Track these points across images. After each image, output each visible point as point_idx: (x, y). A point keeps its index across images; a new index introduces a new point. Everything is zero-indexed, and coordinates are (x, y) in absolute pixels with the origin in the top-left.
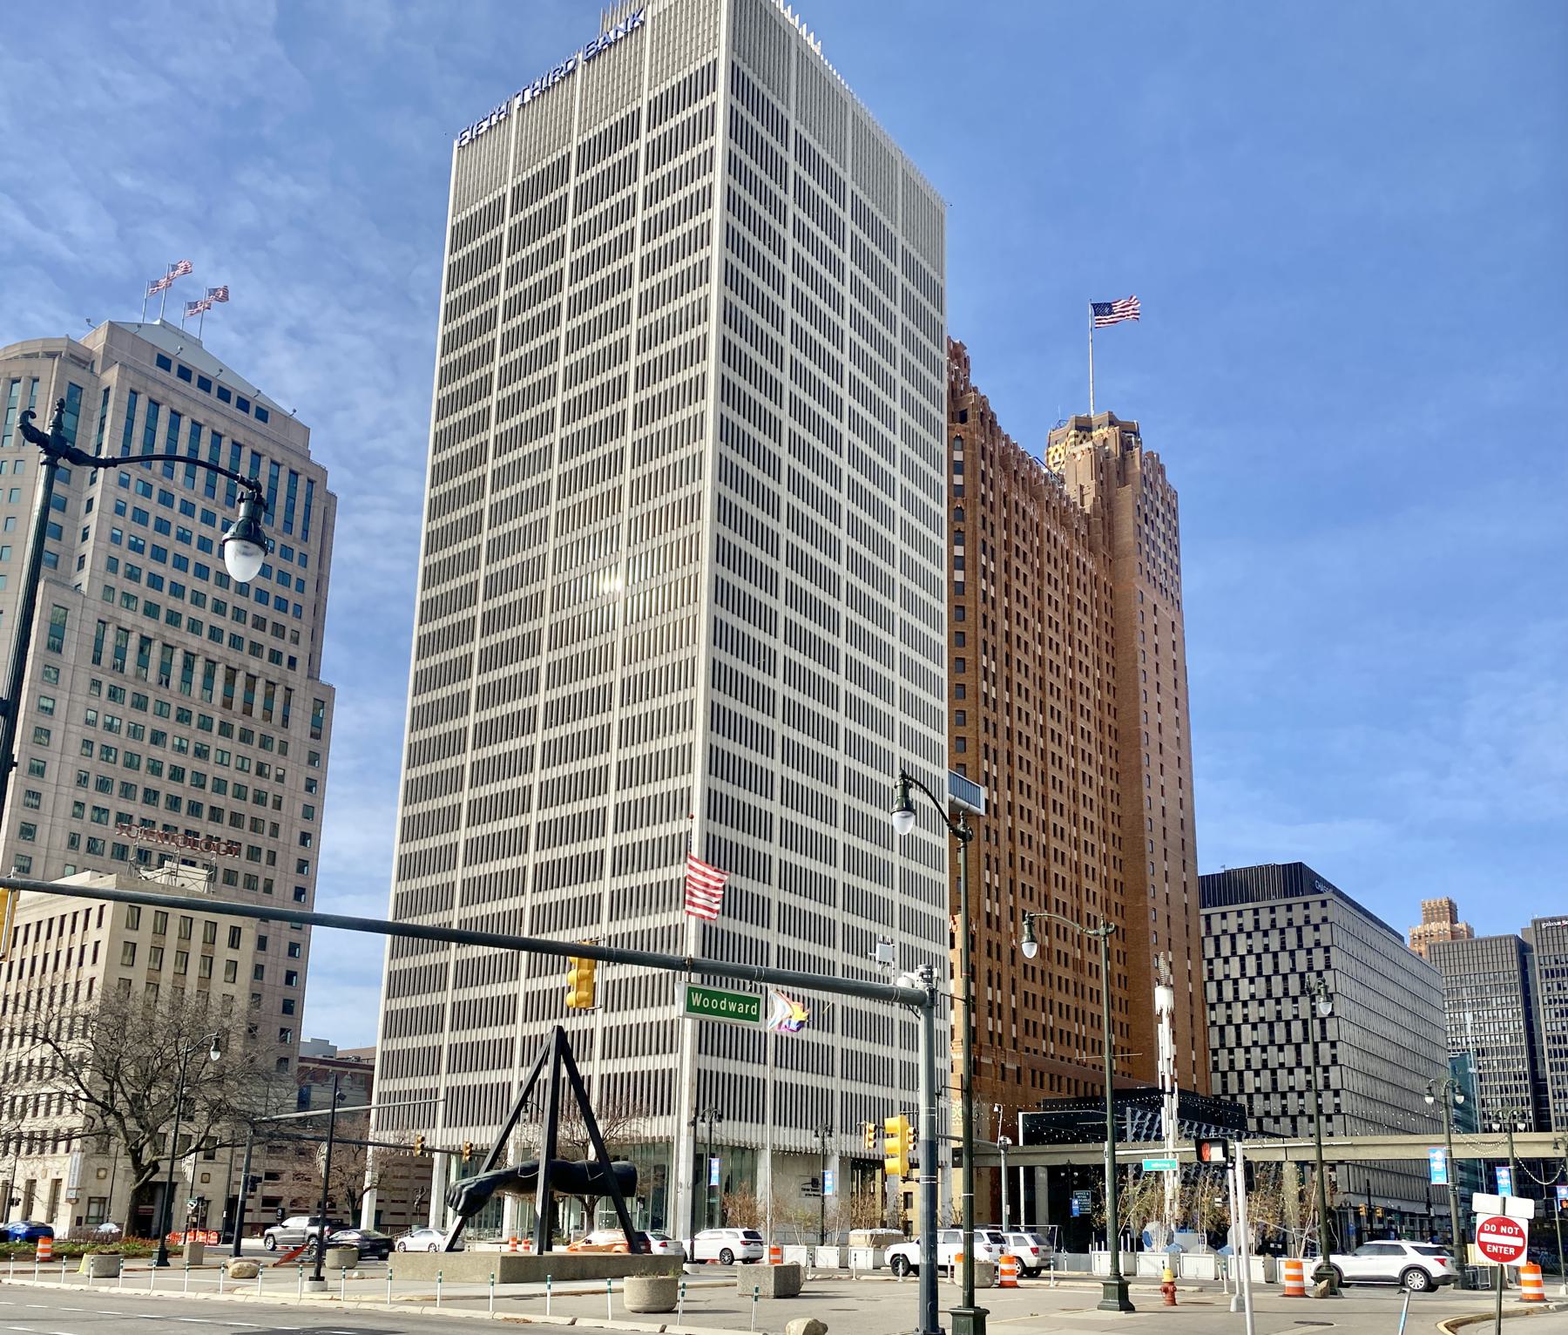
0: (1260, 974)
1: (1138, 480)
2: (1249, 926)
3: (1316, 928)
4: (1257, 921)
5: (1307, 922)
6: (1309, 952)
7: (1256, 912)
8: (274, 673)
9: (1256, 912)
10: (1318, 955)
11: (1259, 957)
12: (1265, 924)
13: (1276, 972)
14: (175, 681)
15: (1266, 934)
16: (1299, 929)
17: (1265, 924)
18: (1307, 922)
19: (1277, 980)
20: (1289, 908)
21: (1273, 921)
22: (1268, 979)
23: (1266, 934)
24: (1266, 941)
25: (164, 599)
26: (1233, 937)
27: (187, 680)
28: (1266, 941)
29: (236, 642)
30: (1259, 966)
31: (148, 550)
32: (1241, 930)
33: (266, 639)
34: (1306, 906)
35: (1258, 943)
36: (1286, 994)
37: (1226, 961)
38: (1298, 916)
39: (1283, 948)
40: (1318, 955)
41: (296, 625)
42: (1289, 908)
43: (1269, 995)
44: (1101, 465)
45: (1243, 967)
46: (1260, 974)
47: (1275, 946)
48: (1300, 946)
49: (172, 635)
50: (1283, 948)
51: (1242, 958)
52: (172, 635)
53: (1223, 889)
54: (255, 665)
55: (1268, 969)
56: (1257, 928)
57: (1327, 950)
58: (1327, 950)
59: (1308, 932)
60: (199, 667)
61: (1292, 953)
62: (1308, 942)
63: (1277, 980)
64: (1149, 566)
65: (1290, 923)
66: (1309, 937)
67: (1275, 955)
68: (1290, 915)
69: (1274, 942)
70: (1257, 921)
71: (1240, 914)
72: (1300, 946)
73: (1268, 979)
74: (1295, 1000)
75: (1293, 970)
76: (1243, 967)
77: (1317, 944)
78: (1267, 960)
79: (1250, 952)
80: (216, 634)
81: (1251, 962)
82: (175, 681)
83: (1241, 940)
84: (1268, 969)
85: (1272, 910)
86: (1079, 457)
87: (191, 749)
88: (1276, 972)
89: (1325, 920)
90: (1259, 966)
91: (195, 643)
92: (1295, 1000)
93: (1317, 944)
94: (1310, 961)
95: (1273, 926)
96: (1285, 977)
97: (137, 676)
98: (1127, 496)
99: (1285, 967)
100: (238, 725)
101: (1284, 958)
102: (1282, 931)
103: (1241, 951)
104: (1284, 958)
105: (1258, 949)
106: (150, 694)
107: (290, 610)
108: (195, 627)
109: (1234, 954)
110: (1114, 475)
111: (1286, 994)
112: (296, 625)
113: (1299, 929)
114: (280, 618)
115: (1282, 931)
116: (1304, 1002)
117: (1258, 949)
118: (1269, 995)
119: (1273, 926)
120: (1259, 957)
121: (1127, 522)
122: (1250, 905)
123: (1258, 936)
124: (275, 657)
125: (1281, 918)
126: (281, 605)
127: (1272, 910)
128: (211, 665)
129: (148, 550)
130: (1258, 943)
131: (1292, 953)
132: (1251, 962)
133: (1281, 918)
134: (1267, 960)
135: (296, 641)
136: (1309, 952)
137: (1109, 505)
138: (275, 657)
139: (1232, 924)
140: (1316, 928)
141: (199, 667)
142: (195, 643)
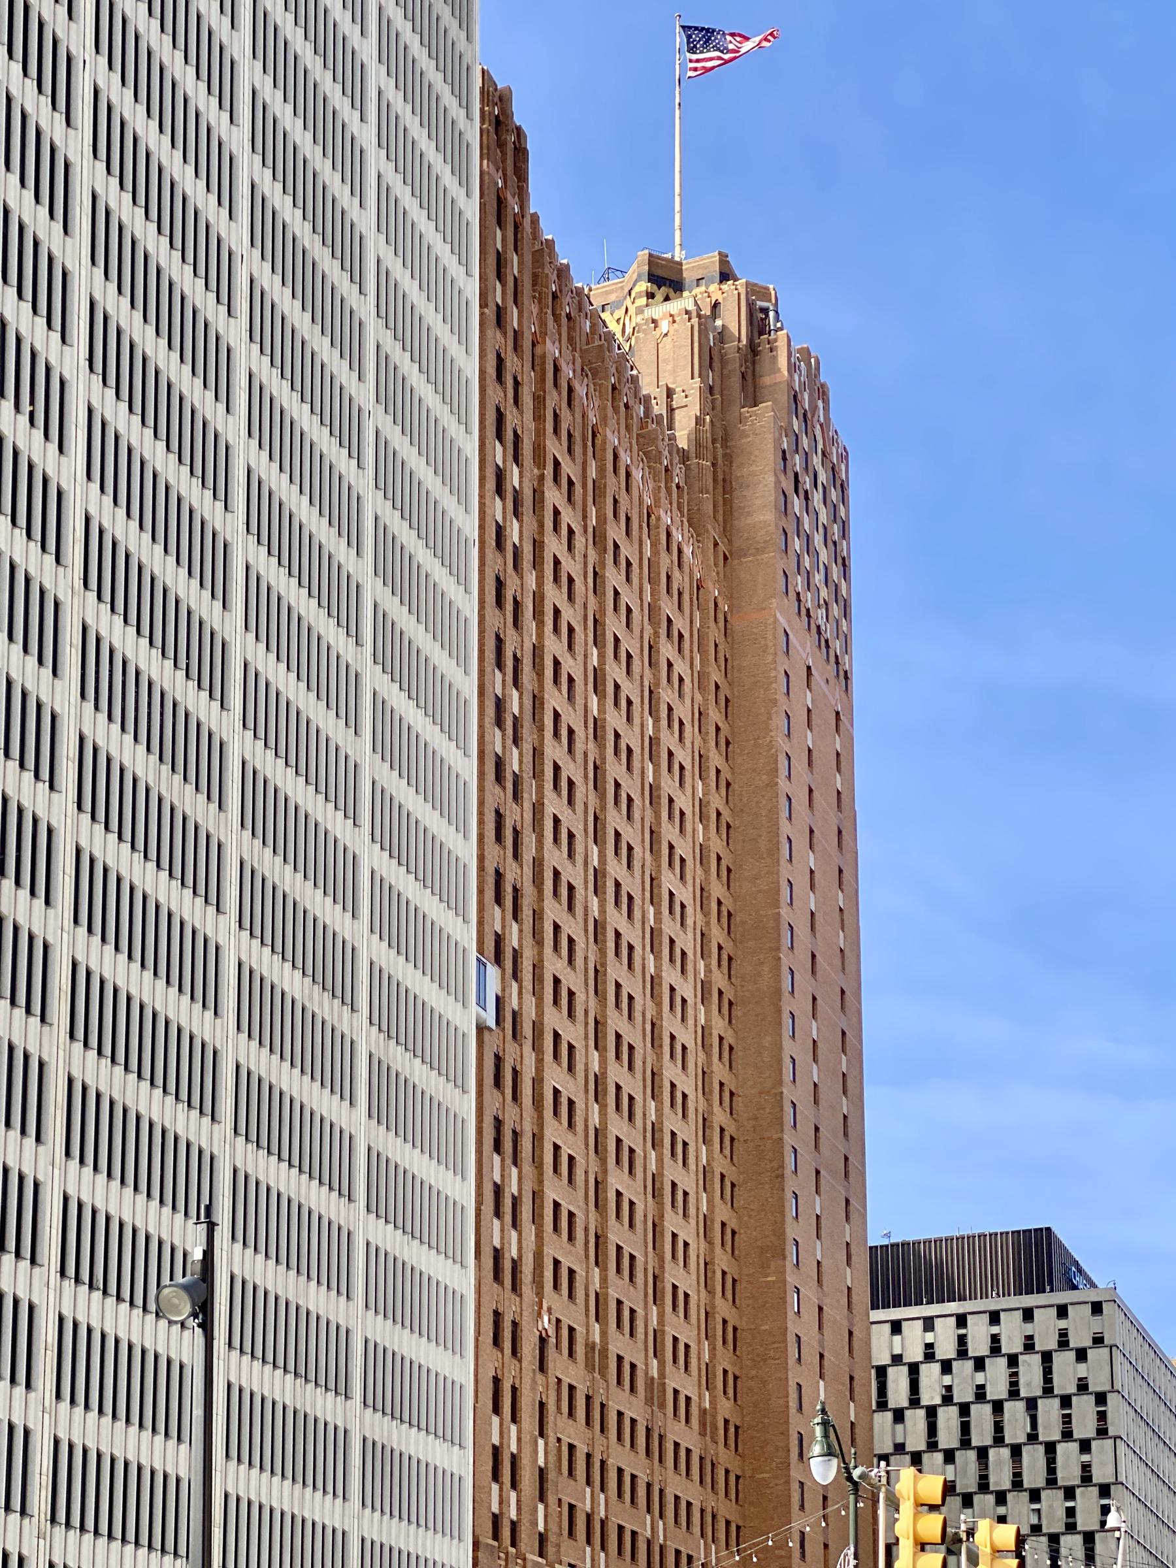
0: (965, 1443)
1: (784, 398)
2: (946, 1349)
3: (1081, 1355)
4: (962, 1340)
5: (1063, 1343)
6: (1066, 1401)
7: (961, 1321)
9: (961, 1321)
10: (1084, 1408)
11: (964, 1409)
12: (978, 1345)
13: (999, 1440)
15: (980, 1364)
16: (1047, 1357)
17: (978, 1345)
18: (1063, 1343)
19: (1000, 1457)
20: (1028, 1315)
21: (995, 1339)
22: (982, 1453)
23: (980, 1364)
24: (980, 1378)
26: (914, 1369)
28: (980, 1378)
30: (965, 1428)
32: (929, 1356)
34: (1062, 1311)
35: (964, 1380)
36: (1017, 1484)
37: (899, 1416)
38: (1045, 1329)
39: (1014, 1393)
40: (1084, 1408)
42: (1028, 1315)
43: (984, 1487)
44: (711, 354)
45: (932, 1430)
46: (965, 1443)
47: (998, 1389)
48: (1048, 1391)
50: (1014, 1393)
51: (931, 1412)
53: (903, 1276)
55: (982, 1434)
56: (962, 1353)
57: (1101, 1398)
58: (1101, 1398)
59: (1064, 1362)
61: (1032, 1404)
62: (1064, 1383)
63: (1000, 1457)
64: (799, 582)
65: (1029, 1346)
66: (1066, 1372)
67: (998, 1407)
68: (1029, 1329)
69: (996, 1378)
70: (962, 1340)
71: (929, 1324)
72: (1048, 1391)
73: (982, 1453)
74: (1035, 1495)
75: (1033, 1438)
76: (932, 1430)
77: (1083, 1386)
78: (982, 1415)
79: (947, 1399)
81: (948, 1418)
83: (930, 1374)
84: (982, 1434)
85: (995, 1318)
86: (664, 326)
88: (999, 1440)
89: (1098, 1341)
90: (965, 1428)
92: (1035, 1495)
93: (1083, 1386)
94: (1067, 1419)
95: (995, 1350)
96: (1016, 1451)
98: (762, 426)
99: (1016, 1431)
101: (1015, 1412)
102: (1013, 1360)
103: (930, 1395)
104: (1015, 1412)
105: (964, 1394)
109: (915, 1402)
110: (735, 381)
111: (1017, 1484)
113: (1047, 1357)
115: (1013, 1360)
116: (1053, 1502)
117: (964, 1394)
118: (984, 1487)
119: (995, 1350)
120: (964, 1409)
121: (761, 483)
122: (954, 1307)
123: (963, 1368)
125: (1012, 1333)
127: (995, 1318)
130: (964, 1380)
131: (1032, 1404)
132: (948, 1418)
133: (1012, 1333)
134: (982, 1415)
136: (1066, 1401)
137: (726, 439)
139: (912, 1344)
140: (1081, 1355)
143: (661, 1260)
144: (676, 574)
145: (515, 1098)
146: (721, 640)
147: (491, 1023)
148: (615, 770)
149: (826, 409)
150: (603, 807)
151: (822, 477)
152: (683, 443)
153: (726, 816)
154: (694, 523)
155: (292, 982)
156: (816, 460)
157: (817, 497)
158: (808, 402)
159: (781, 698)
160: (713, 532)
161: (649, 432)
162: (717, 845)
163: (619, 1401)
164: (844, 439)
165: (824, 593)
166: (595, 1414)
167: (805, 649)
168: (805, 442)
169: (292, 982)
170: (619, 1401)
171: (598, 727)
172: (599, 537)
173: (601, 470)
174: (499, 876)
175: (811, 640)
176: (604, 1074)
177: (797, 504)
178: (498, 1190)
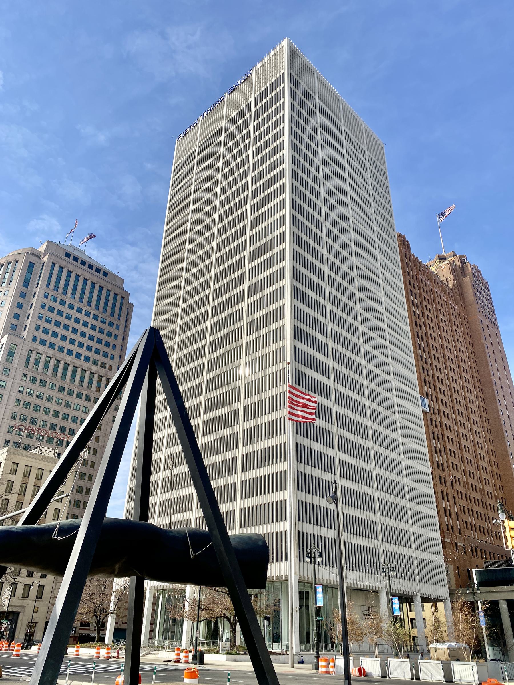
8: (102, 372)
14: (59, 375)
25: (58, 341)
27: (64, 375)
29: (87, 359)
31: (53, 322)
33: (99, 358)
41: (113, 352)
49: (60, 356)
52: (60, 356)
54: (94, 369)
60: (70, 369)
80: (78, 356)
82: (59, 375)
87: (63, 404)
91: (69, 359)
97: (43, 372)
100: (85, 393)
106: (48, 380)
107: (111, 347)
108: (70, 353)
112: (113, 352)
114: (107, 350)
124: (103, 365)
126: (107, 344)
128: (75, 368)
129: (53, 322)
135: (112, 359)
138: (103, 365)
141: (70, 369)
142: (69, 359)
143: (478, 460)
144: (454, 312)
145: (436, 427)
146: (467, 323)
147: (428, 411)
148: (447, 354)
149: (481, 275)
150: (446, 362)
151: (483, 288)
152: (451, 288)
153: (475, 359)
154: (456, 302)
155: (381, 410)
156: (481, 285)
157: (482, 292)
158: (477, 274)
159: (483, 333)
160: (461, 303)
161: (443, 287)
162: (474, 365)
163: (473, 494)
164: (486, 279)
165: (488, 310)
166: (468, 498)
167: (486, 322)
168: (477, 282)
169: (381, 410)
170: (473, 494)
171: (442, 346)
172: (436, 309)
173: (434, 296)
174: (425, 380)
175: (487, 320)
176: (457, 419)
177: (478, 294)
178: (435, 448)
